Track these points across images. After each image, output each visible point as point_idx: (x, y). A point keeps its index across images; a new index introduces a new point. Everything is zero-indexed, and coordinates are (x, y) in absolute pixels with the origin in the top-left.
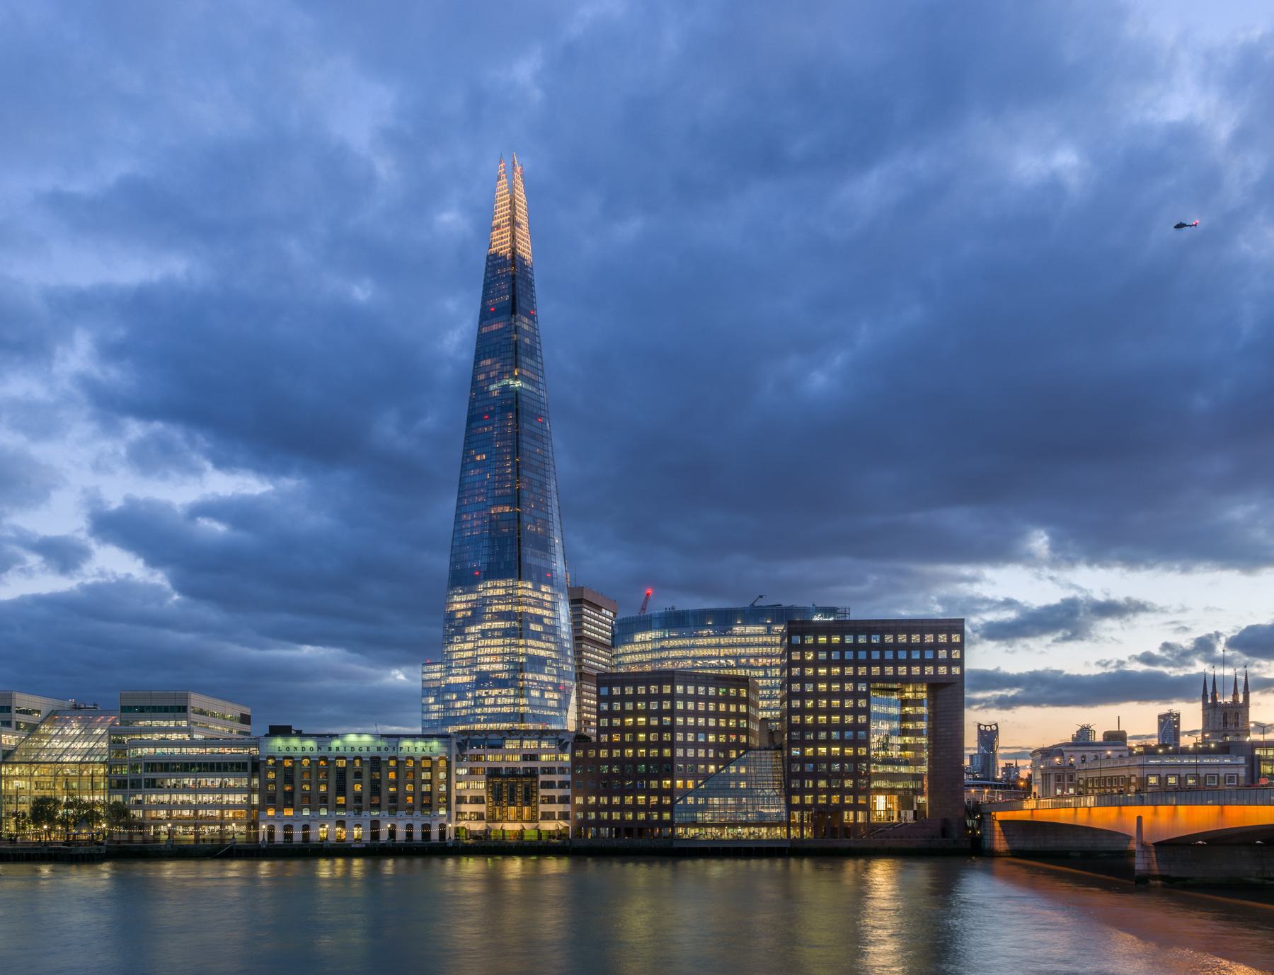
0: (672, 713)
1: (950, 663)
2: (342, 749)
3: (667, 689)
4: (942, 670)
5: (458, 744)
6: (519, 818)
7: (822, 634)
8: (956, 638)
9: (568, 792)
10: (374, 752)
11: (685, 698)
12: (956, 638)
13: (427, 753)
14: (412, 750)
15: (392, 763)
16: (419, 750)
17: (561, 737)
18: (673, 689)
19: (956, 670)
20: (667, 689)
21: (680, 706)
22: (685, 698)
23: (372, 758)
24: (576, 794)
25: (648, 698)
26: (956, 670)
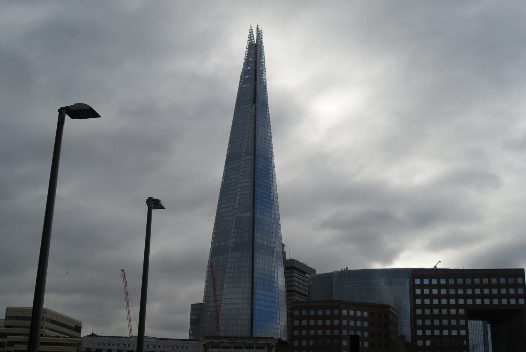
3: (336, 312)
4: (513, 301)
5: (204, 345)
12: (520, 280)
18: (340, 312)
20: (336, 312)
21: (345, 322)
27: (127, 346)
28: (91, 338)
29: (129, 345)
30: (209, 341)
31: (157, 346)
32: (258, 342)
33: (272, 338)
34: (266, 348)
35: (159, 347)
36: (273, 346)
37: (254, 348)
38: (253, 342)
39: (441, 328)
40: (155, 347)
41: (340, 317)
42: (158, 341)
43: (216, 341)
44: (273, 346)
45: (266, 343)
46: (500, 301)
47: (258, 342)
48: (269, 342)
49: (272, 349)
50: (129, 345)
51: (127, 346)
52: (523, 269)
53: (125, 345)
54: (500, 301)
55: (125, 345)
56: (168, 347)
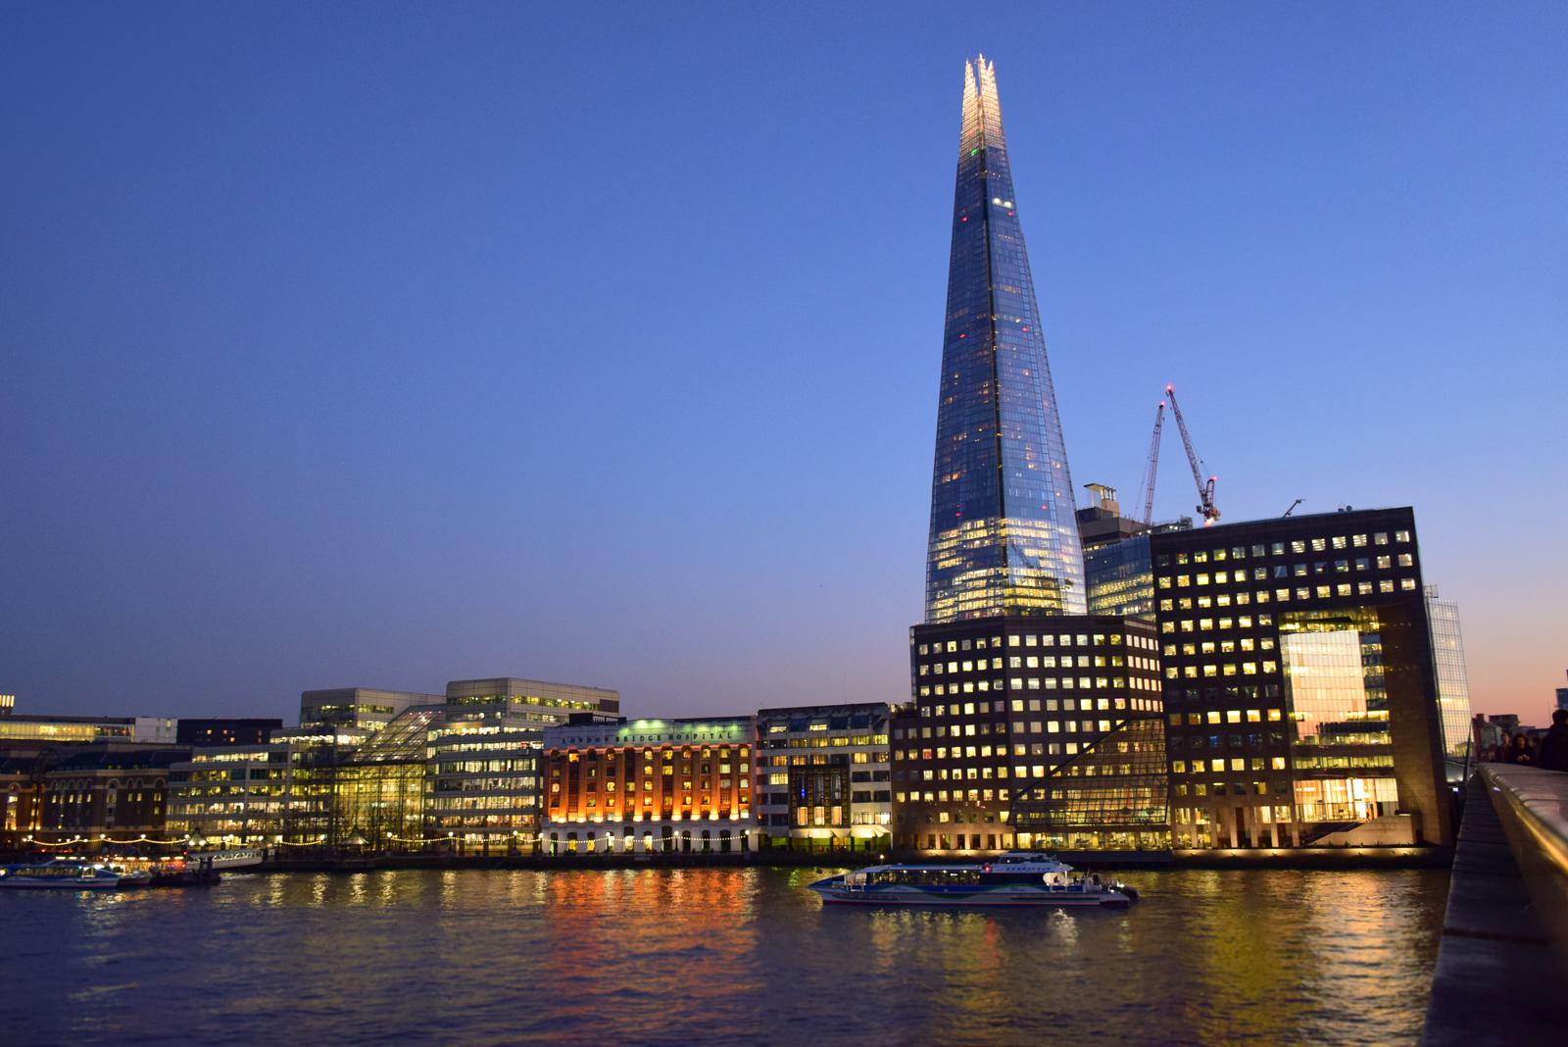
0: (1006, 674)
1: (1397, 573)
2: (630, 738)
5: (758, 727)
6: (828, 822)
7: (1200, 550)
8: (1403, 537)
9: (886, 786)
11: (1024, 651)
12: (1403, 537)
13: (725, 740)
14: (708, 737)
15: (648, 755)
16: (716, 736)
17: (876, 712)
18: (1005, 642)
19: (1409, 584)
24: (897, 789)
26: (1409, 584)
28: (559, 730)
30: (765, 719)
32: (857, 714)
34: (870, 726)
36: (883, 721)
37: (849, 727)
38: (847, 713)
39: (1200, 660)
41: (1005, 652)
45: (871, 714)
47: (857, 714)
48: (876, 713)
49: (882, 726)
52: (1410, 510)
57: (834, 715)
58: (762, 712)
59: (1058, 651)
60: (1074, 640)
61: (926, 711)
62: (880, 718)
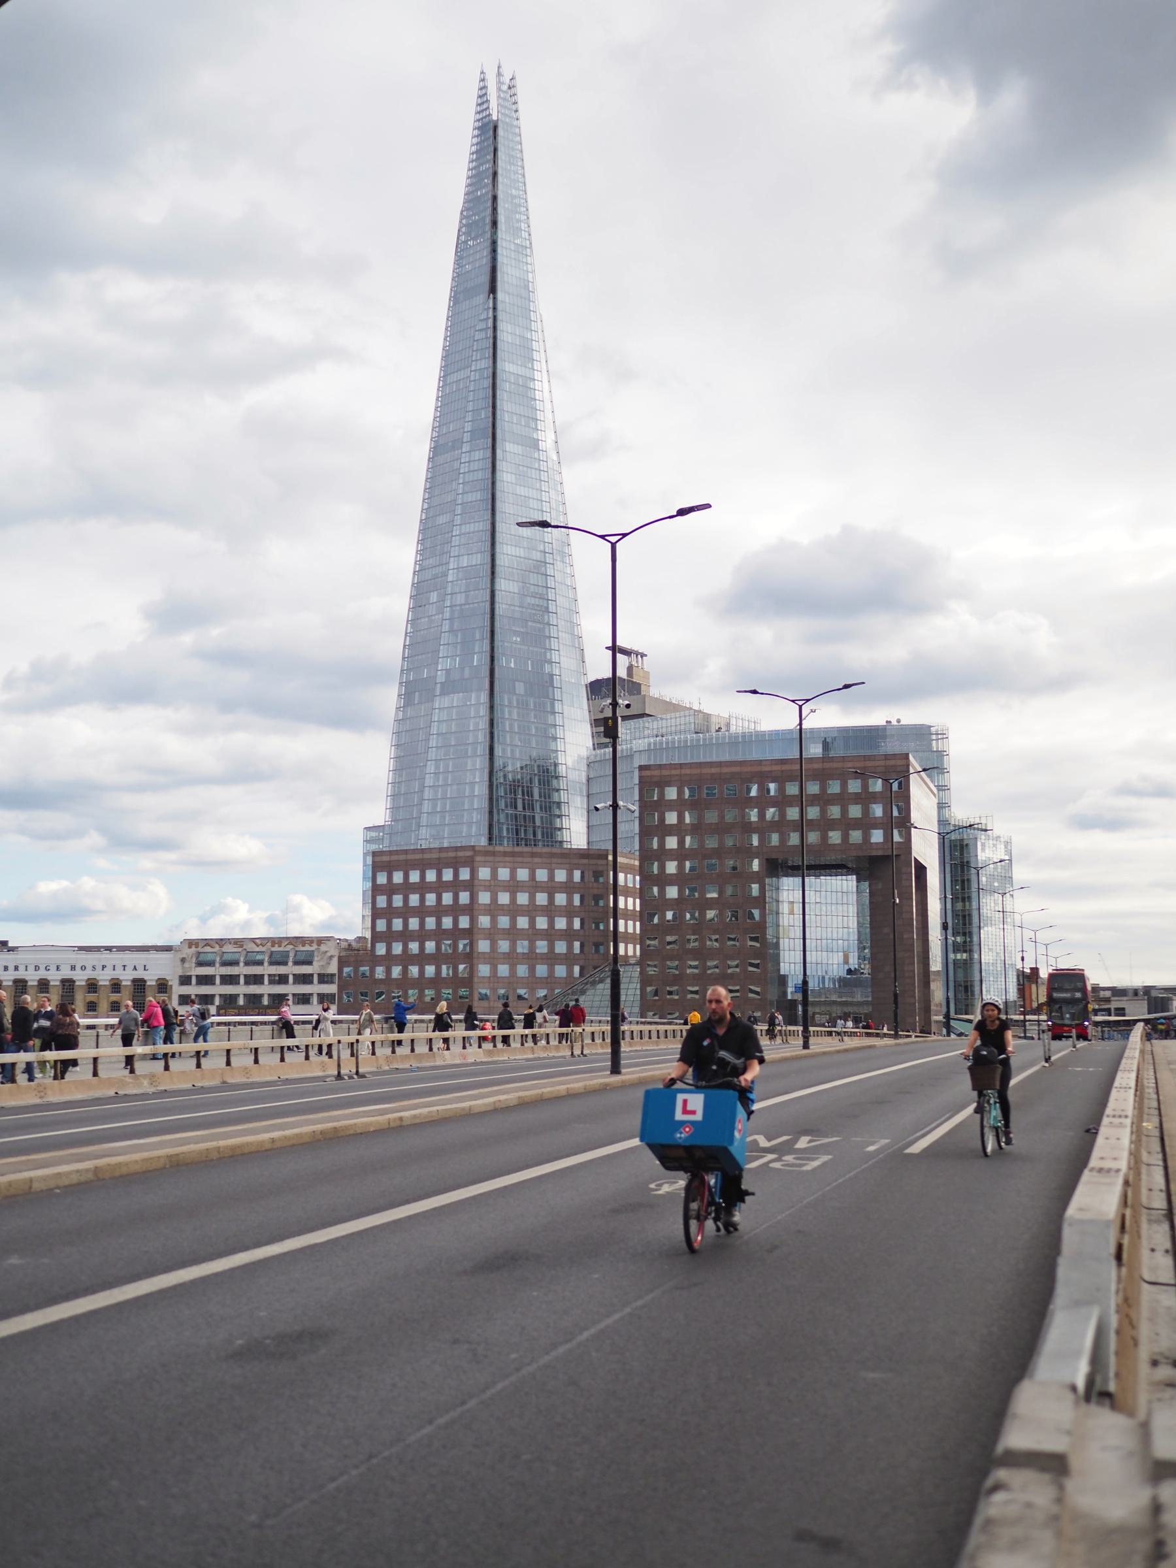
10: (66, 973)
18: (473, 873)
21: (484, 898)
22: (494, 886)
23: (63, 981)
25: (439, 887)
27: (11, 968)
29: (16, 968)
31: (78, 968)
33: (328, 939)
35: (83, 968)
36: (331, 957)
37: (290, 964)
40: (73, 968)
42: (84, 955)
43: (208, 949)
44: (331, 957)
46: (845, 837)
50: (16, 968)
51: (11, 968)
53: (6, 968)
54: (845, 837)
55: (6, 968)
56: (104, 967)
57: (273, 949)
58: (191, 943)
59: (533, 887)
60: (551, 876)
61: (381, 949)
62: (329, 954)
